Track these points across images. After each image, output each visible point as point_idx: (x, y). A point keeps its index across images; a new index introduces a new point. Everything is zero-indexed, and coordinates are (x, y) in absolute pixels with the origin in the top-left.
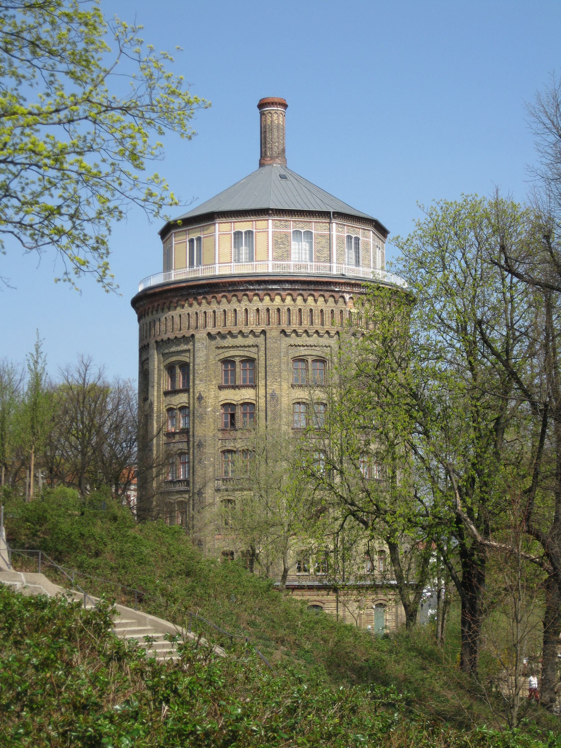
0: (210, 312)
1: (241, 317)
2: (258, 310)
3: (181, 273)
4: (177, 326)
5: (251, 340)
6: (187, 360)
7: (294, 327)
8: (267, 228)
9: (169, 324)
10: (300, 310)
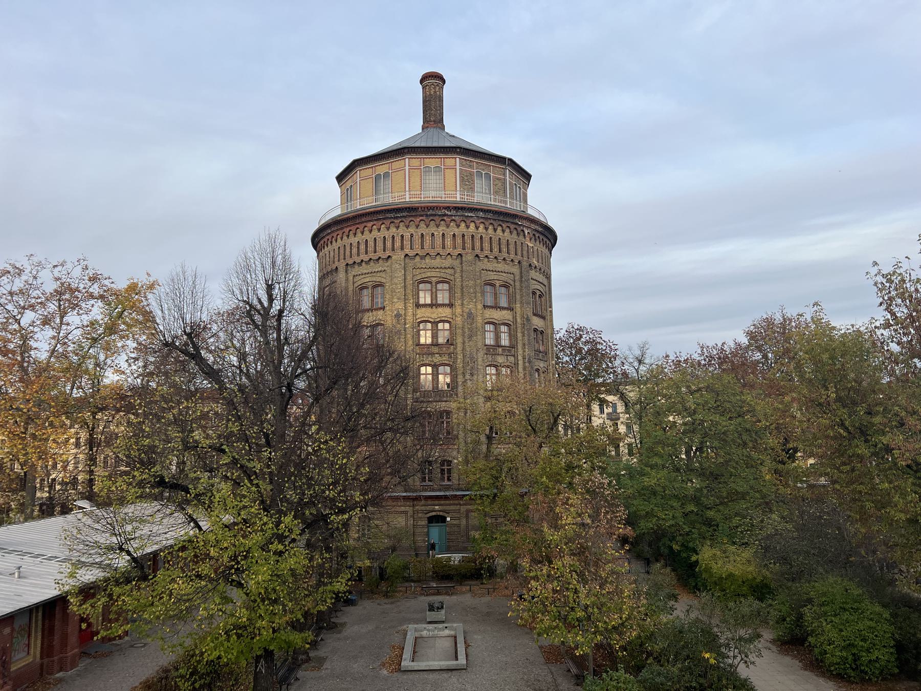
0: (407, 235)
2: (454, 235)
4: (371, 249)
5: (448, 262)
6: (383, 280)
7: (487, 252)
9: (362, 247)
10: (491, 238)
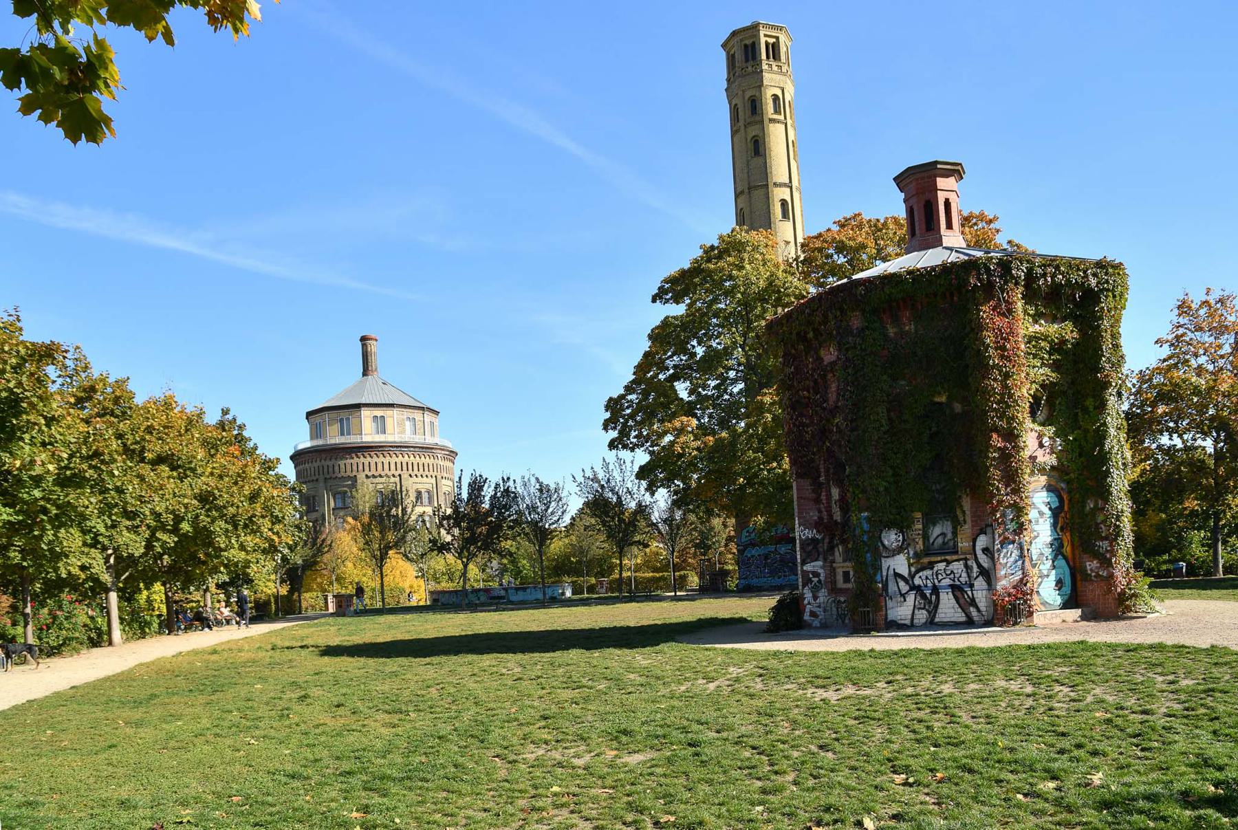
1: (386, 466)
3: (334, 437)
8: (392, 416)
